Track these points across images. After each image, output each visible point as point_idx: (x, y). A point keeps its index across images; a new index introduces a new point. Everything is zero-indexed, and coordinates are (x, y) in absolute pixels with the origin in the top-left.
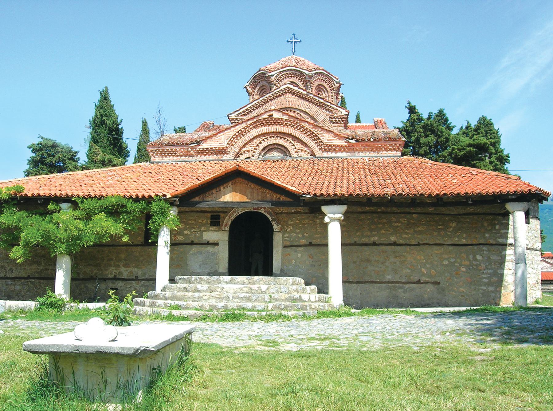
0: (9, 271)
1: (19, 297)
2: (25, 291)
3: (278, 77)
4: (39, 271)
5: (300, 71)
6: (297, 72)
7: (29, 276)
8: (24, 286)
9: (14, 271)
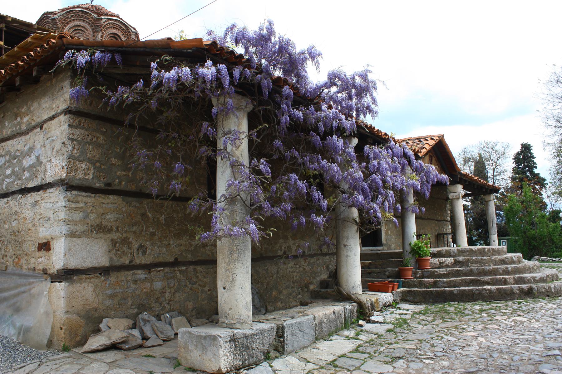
0: (138, 250)
1: (161, 304)
2: (173, 290)
3: (106, 23)
4: (193, 248)
5: (126, 26)
6: (123, 27)
7: (176, 259)
8: (169, 281)
9: (148, 251)
